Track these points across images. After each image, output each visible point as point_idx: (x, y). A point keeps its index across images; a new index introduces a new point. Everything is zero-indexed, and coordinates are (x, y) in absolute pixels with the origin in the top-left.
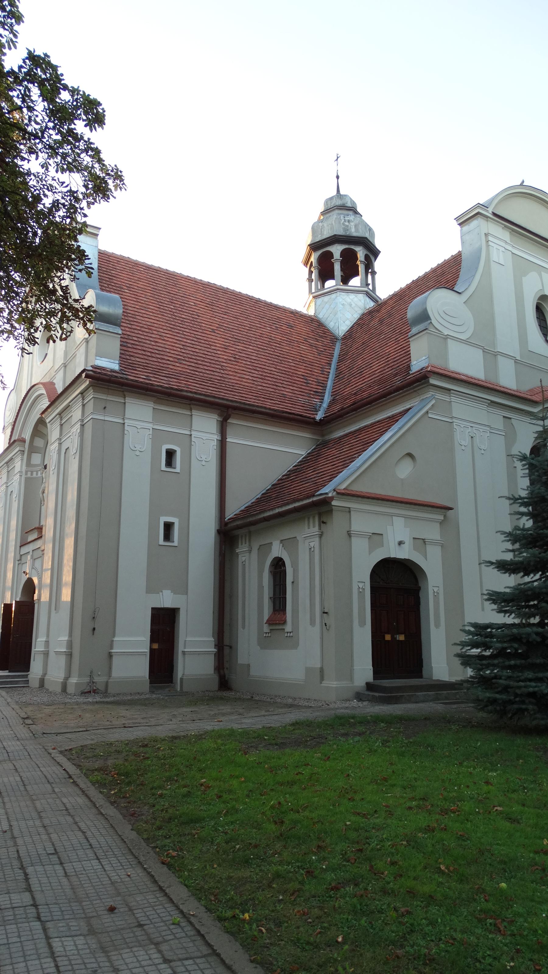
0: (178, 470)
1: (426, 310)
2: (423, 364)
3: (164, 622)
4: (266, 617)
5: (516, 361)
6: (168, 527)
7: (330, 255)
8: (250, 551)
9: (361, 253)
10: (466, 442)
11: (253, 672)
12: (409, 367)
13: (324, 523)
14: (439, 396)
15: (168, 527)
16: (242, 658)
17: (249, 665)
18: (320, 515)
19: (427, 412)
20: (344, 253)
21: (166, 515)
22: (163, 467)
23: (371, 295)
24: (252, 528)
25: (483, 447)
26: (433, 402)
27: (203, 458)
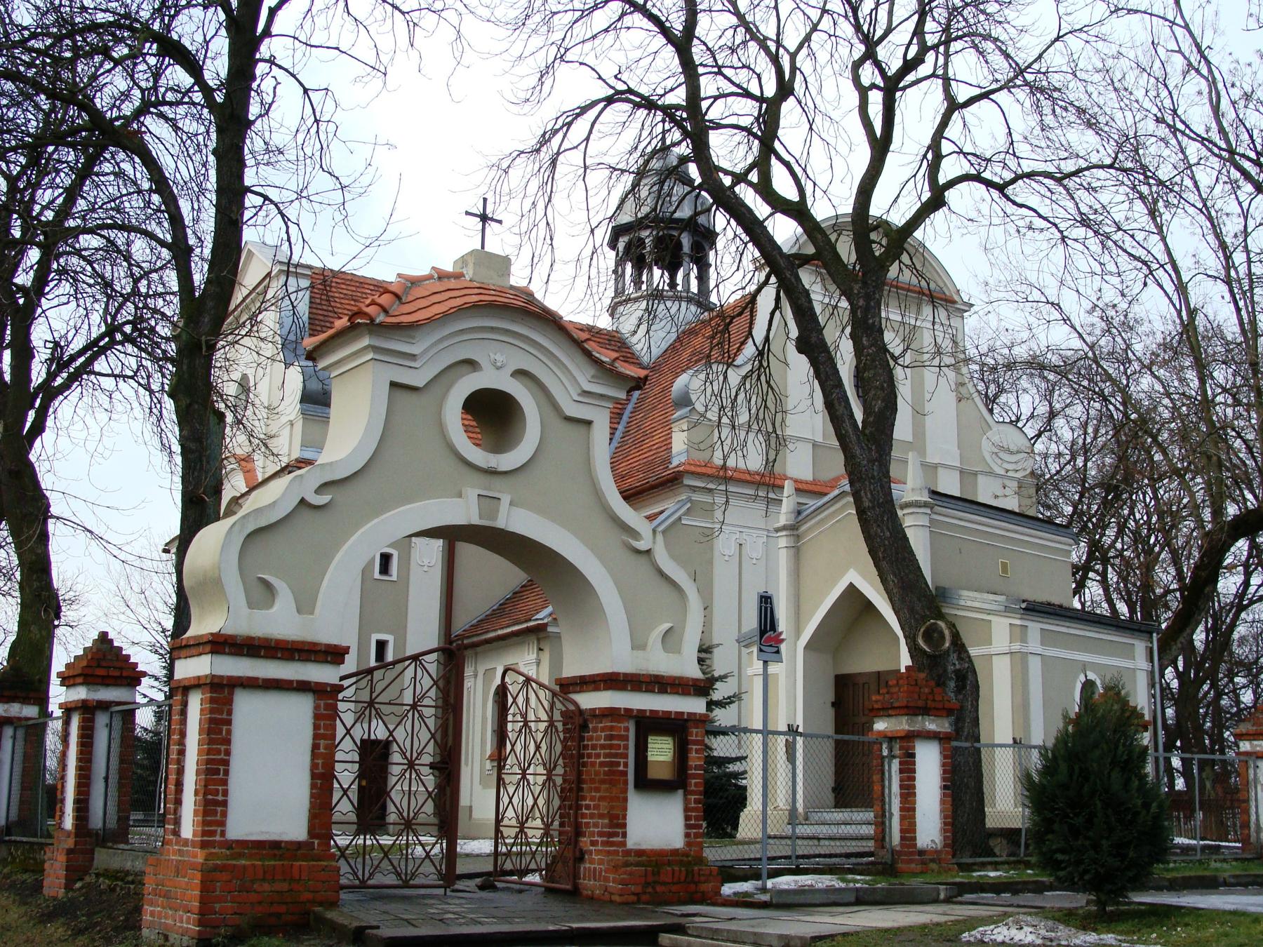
0: (394, 578)
1: (687, 394)
2: (683, 459)
3: (374, 756)
4: (488, 753)
5: (815, 445)
6: (381, 645)
7: (641, 242)
8: (476, 676)
9: (686, 241)
10: (733, 549)
11: (476, 815)
12: (668, 460)
13: (541, 650)
14: (697, 497)
15: (381, 645)
16: (464, 801)
17: (471, 807)
18: (539, 640)
19: (680, 519)
20: (658, 241)
21: (379, 632)
22: (377, 575)
23: (701, 299)
24: (478, 649)
25: (754, 556)
26: (689, 505)
27: (426, 563)
